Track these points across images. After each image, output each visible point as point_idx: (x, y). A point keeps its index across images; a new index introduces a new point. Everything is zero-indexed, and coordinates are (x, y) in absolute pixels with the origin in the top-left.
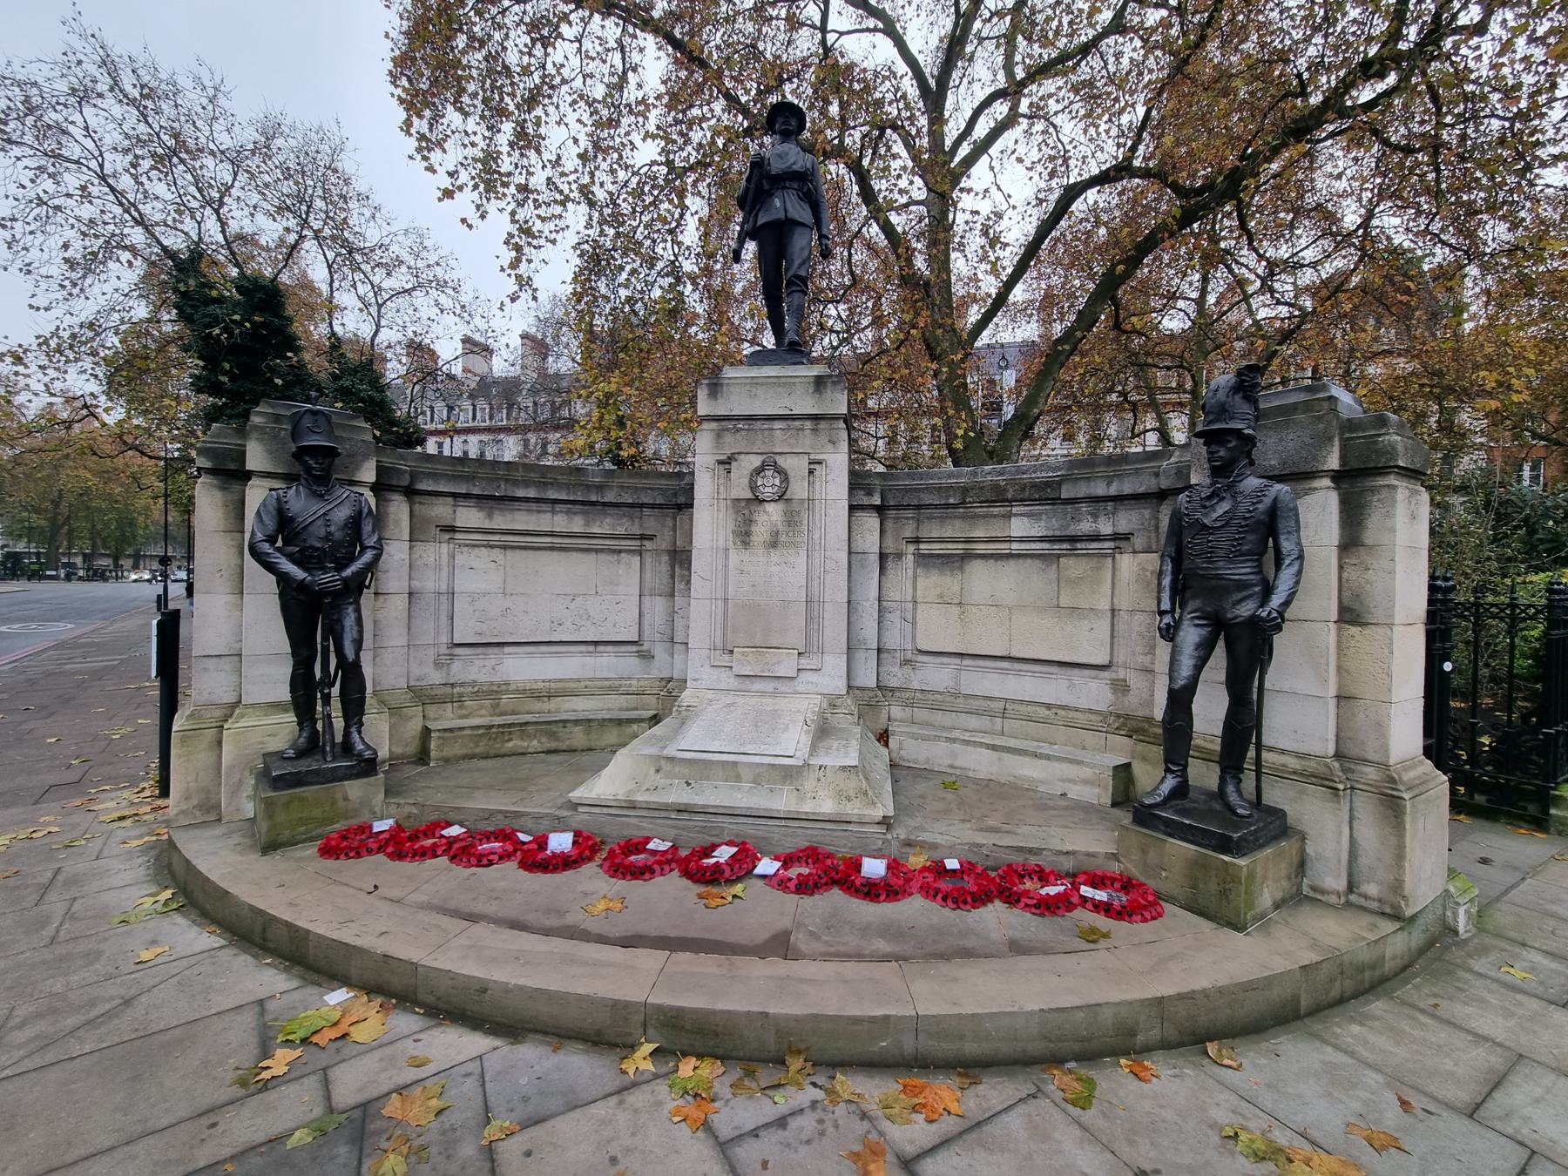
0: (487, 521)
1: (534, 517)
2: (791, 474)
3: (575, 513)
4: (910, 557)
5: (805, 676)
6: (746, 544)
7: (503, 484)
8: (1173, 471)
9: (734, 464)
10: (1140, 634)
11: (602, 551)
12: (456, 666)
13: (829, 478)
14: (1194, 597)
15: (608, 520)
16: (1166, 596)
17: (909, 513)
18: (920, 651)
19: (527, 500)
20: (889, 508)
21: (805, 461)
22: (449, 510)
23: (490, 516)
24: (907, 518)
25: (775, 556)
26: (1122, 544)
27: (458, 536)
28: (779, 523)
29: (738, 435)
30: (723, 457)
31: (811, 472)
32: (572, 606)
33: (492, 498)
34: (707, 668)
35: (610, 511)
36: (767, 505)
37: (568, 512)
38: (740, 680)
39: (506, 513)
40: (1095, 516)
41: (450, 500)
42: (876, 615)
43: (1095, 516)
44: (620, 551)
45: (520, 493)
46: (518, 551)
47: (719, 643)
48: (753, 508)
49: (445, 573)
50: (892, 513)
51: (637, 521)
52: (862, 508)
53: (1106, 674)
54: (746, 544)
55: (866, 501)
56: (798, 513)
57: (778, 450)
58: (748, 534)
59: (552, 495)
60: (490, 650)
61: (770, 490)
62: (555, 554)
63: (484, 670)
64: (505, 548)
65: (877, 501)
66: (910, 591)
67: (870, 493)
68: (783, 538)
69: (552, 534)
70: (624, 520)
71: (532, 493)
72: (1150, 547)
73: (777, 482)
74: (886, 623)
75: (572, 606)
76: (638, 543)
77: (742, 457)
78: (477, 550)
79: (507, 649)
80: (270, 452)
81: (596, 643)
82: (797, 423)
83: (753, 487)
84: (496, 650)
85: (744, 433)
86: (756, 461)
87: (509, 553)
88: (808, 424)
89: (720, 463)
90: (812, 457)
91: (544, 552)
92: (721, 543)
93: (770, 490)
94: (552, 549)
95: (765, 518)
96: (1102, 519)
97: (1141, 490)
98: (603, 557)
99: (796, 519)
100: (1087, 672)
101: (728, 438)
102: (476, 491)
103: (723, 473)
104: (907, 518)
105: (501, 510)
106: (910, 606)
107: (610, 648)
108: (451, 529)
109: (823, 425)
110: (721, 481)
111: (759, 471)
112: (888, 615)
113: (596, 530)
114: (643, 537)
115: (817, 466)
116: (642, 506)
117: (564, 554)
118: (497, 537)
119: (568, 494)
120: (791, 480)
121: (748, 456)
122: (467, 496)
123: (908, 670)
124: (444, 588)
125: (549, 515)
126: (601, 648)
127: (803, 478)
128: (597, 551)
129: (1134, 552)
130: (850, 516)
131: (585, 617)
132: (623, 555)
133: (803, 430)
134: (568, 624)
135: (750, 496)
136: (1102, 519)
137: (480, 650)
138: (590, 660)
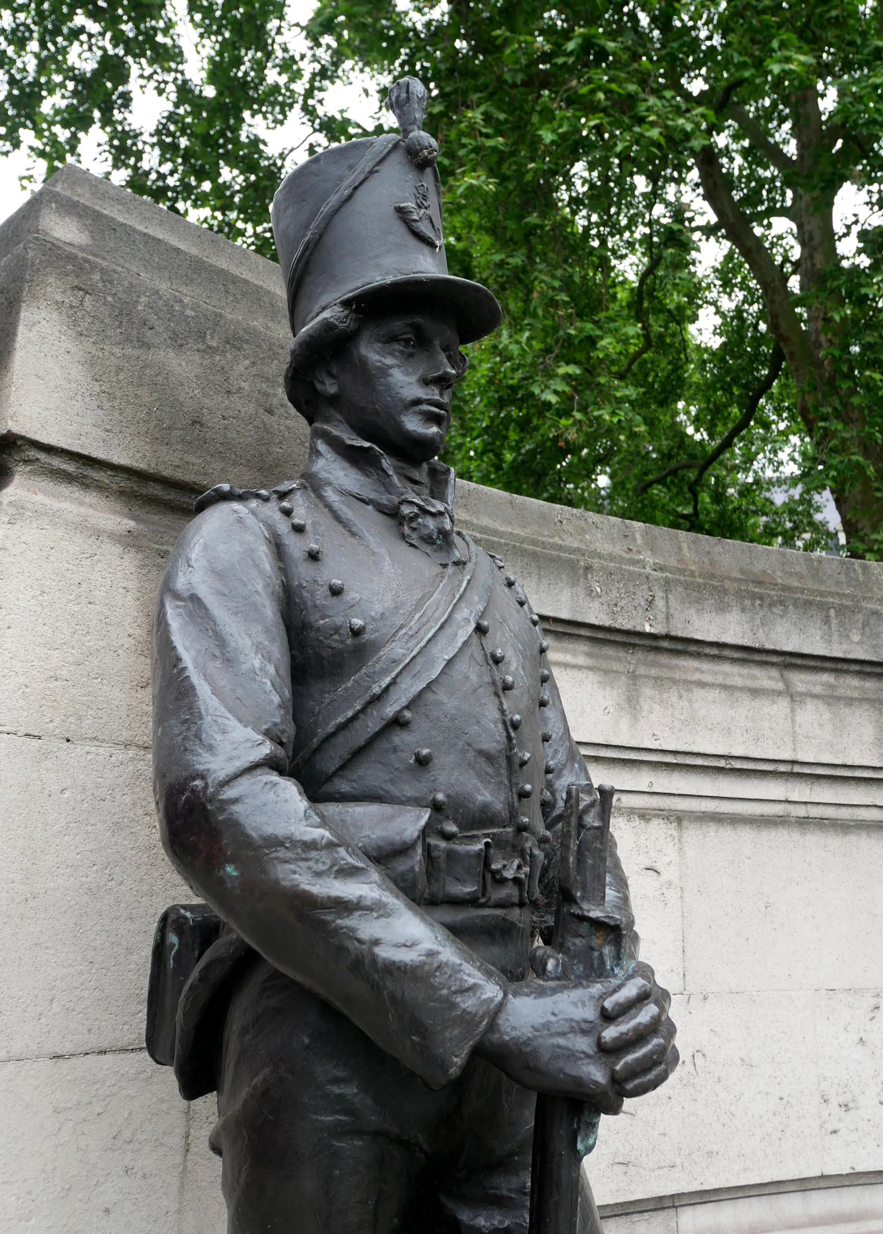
0: (625, 723)
3: (850, 701)
23: (632, 703)
37: (831, 699)
62: (813, 840)
64: (679, 818)
80: (91, 362)
87: (693, 834)
102: (596, 615)
117: (834, 842)
125: (783, 704)
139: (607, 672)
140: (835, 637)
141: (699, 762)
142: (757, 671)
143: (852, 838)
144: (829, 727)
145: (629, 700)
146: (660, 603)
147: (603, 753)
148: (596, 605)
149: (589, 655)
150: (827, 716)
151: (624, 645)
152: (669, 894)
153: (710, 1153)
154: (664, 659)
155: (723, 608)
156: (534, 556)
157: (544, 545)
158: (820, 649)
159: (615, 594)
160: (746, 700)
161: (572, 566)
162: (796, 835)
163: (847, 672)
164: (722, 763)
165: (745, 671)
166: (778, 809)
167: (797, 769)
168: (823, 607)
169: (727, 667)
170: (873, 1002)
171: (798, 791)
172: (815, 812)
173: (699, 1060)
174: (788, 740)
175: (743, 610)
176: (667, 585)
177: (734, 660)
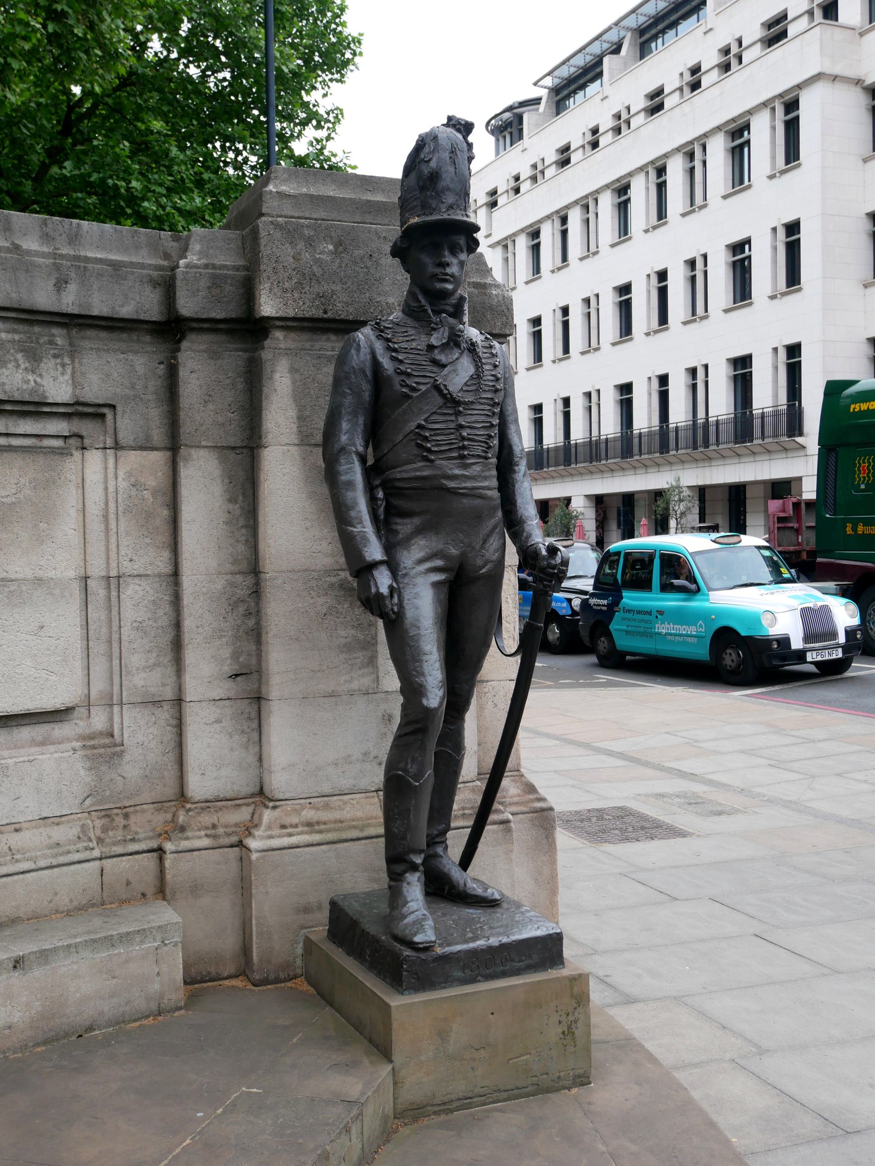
8: (204, 283)
10: (139, 627)
14: (419, 531)
16: (367, 528)
26: (85, 427)
40: (34, 357)
43: (34, 357)
53: (59, 730)
72: (148, 438)
96: (49, 365)
97: (126, 311)
100: (25, 733)
129: (117, 446)
136: (49, 365)
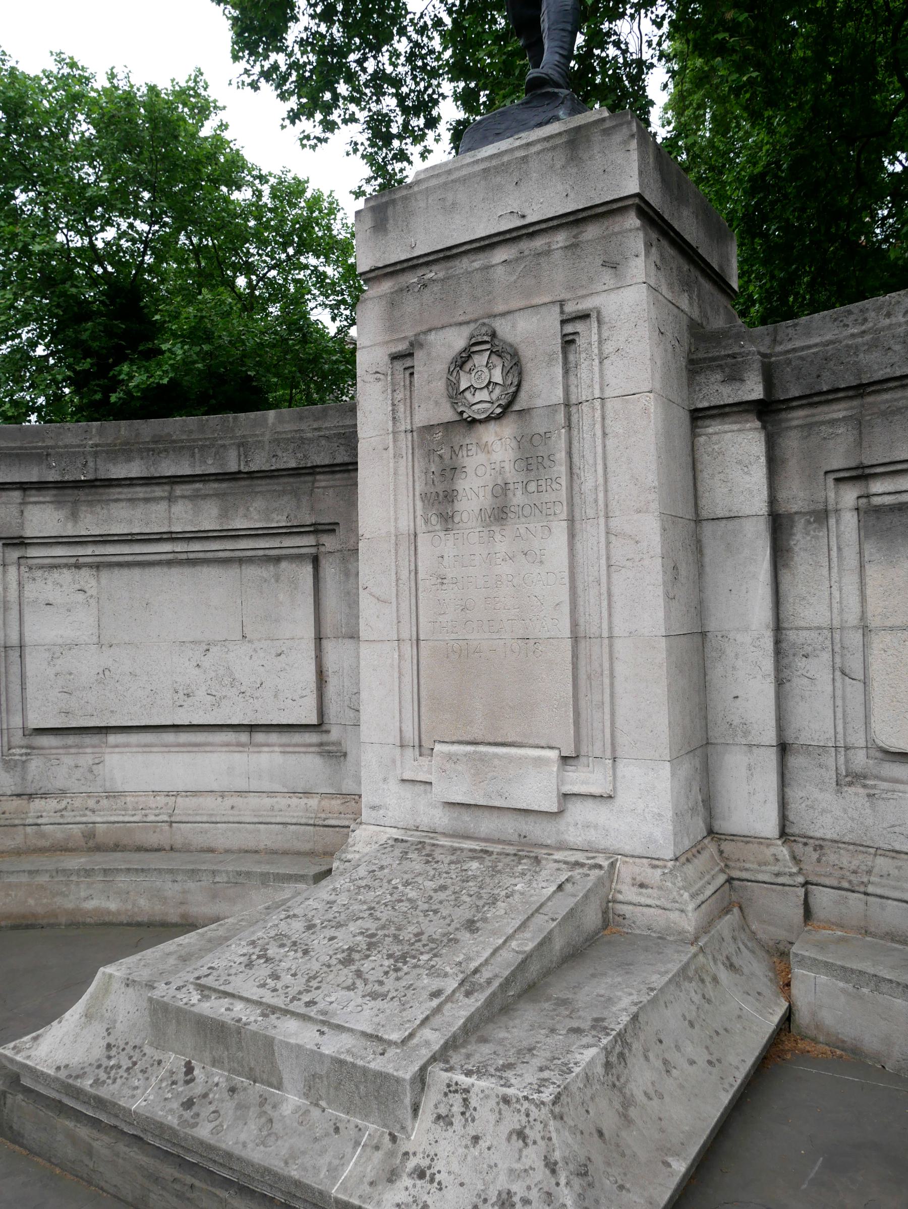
0: (70, 525)
1: (139, 511)
2: (526, 353)
3: (205, 497)
4: (850, 520)
5: (578, 812)
6: (447, 520)
7: (91, 460)
9: (419, 355)
11: (250, 560)
12: (35, 765)
13: (609, 348)
15: (259, 503)
17: (838, 411)
18: (886, 752)
19: (130, 482)
20: (788, 404)
21: (553, 318)
22: (14, 510)
23: (74, 516)
24: (832, 422)
25: (502, 544)
27: (32, 552)
28: (508, 466)
29: (427, 296)
30: (401, 347)
31: (568, 342)
32: (206, 662)
33: (77, 485)
34: (394, 786)
35: (262, 485)
36: (481, 428)
37: (195, 497)
38: (455, 812)
39: (98, 509)
41: (16, 495)
42: (768, 665)
44: (278, 559)
45: (119, 471)
46: (116, 571)
47: (410, 734)
48: (457, 439)
49: (14, 614)
50: (798, 417)
51: (305, 500)
52: (721, 412)
54: (447, 520)
55: (728, 394)
56: (546, 436)
57: (500, 308)
58: (449, 497)
59: (168, 468)
60: (88, 740)
61: (483, 395)
63: (78, 774)
64: (98, 566)
65: (754, 390)
66: (853, 602)
67: (734, 377)
68: (518, 498)
69: (171, 537)
70: (286, 498)
71: (135, 469)
73: (497, 377)
74: (798, 684)
75: (206, 662)
76: (310, 540)
77: (432, 337)
78: (56, 574)
79: (112, 739)
81: (252, 728)
82: (539, 243)
83: (455, 394)
84: (95, 739)
85: (436, 288)
86: (457, 340)
87: (105, 575)
88: (560, 239)
89: (395, 357)
90: (570, 308)
91: (158, 570)
92: (405, 524)
93: (483, 395)
94: (169, 563)
95: (481, 458)
98: (252, 572)
99: (542, 451)
101: (410, 305)
103: (400, 376)
104: (832, 422)
105: (90, 503)
106: (855, 639)
107: (274, 737)
108: (19, 542)
109: (592, 231)
110: (399, 396)
111: (462, 361)
112: (801, 663)
113: (239, 523)
114: (317, 529)
115: (579, 327)
116: (313, 471)
117: (188, 571)
118: (89, 550)
119: (192, 465)
120: (529, 366)
121: (441, 334)
122: (41, 486)
123: (855, 794)
124: (14, 639)
126: (260, 737)
127: (550, 361)
128: (241, 561)
130: (694, 435)
131: (227, 681)
132: (284, 565)
133: (548, 252)
134: (201, 693)
135: (448, 414)
137: (71, 740)
138: (239, 759)
139: (59, 502)
140: (197, 463)
141: (116, 538)
142: (156, 488)
143: (199, 568)
144: (191, 512)
145: (73, 514)
146: (91, 464)
147: (60, 540)
148: (53, 471)
149: (55, 496)
150: (190, 506)
151: (76, 487)
152: (91, 601)
153: (112, 712)
154: (101, 490)
155: (129, 460)
156: (17, 455)
157: (26, 448)
158: (188, 471)
159: (64, 464)
160: (142, 505)
161: (39, 455)
162: (165, 569)
163: (209, 481)
164: (129, 537)
165: (148, 489)
166: (170, 556)
167: (174, 536)
168: (191, 449)
169: (138, 489)
170: (206, 647)
171: (179, 547)
172: (191, 556)
173: (107, 672)
174: (166, 522)
175: (142, 459)
176: (96, 455)
177: (141, 485)
